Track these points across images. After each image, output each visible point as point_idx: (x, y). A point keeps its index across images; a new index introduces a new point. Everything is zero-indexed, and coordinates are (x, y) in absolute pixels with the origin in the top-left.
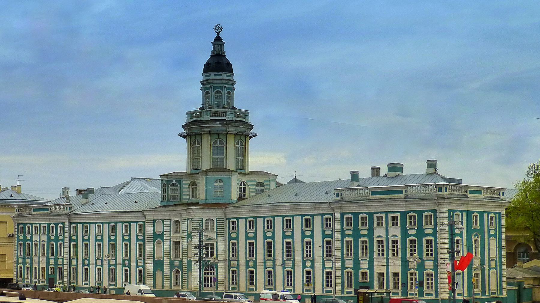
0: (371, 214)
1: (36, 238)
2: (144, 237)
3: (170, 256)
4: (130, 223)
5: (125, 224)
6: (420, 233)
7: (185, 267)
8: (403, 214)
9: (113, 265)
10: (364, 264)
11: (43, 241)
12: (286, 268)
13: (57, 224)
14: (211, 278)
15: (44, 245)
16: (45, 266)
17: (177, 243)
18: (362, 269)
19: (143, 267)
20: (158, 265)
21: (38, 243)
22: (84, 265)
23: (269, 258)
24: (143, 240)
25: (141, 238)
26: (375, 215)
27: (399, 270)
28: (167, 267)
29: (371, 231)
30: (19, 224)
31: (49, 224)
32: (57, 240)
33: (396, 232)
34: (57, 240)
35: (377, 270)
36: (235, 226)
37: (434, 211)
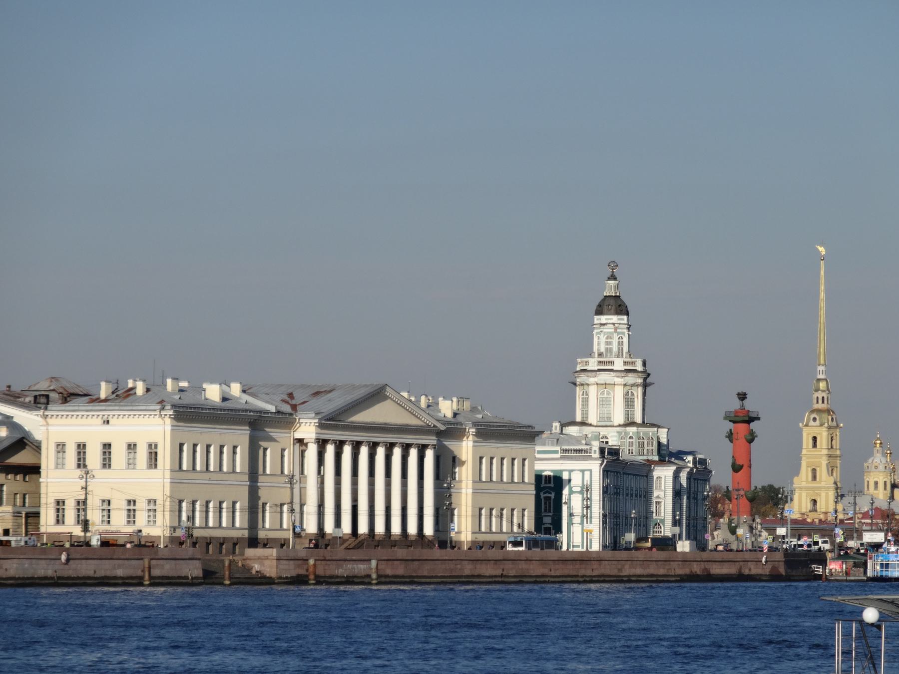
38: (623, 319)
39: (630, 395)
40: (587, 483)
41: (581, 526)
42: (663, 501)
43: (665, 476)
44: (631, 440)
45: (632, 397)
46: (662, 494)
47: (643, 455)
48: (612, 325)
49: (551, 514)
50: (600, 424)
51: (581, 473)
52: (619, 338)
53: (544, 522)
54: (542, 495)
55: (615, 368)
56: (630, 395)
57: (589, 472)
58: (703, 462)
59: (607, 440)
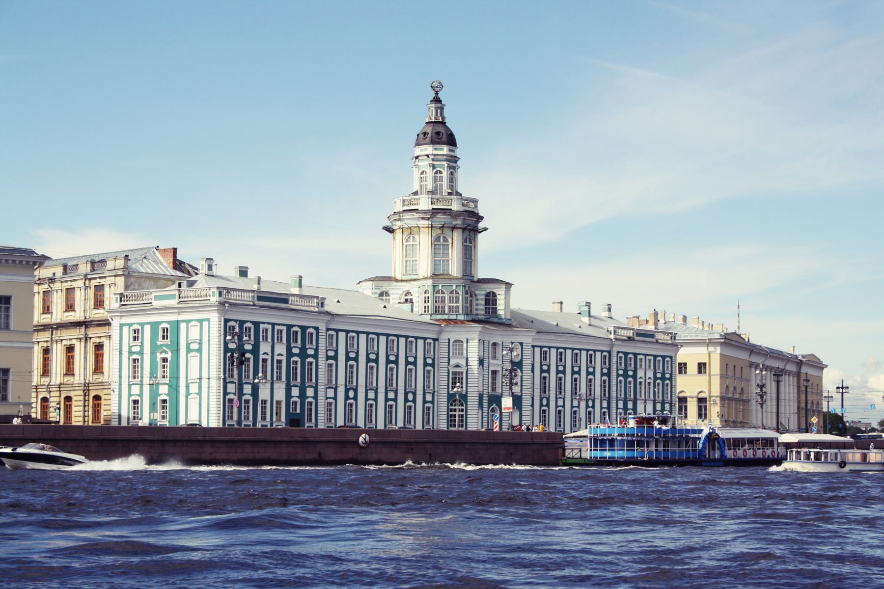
0: (635, 355)
1: (265, 348)
2: (434, 360)
4: (416, 338)
9: (391, 400)
11: (279, 355)
13: (304, 328)
15: (279, 362)
17: (494, 373)
18: (629, 409)
19: (432, 402)
21: (269, 357)
23: (560, 396)
24: (433, 365)
25: (429, 361)
26: (639, 357)
29: (635, 372)
31: (289, 327)
32: (303, 355)
34: (303, 355)
37: (671, 357)
38: (442, 149)
39: (442, 240)
40: (789, 379)
41: (198, 397)
42: (465, 372)
44: (427, 295)
45: (444, 243)
46: (463, 362)
47: (443, 313)
48: (426, 157)
49: (168, 382)
50: (405, 278)
52: (436, 173)
53: (160, 393)
54: (159, 356)
55: (420, 208)
56: (442, 240)
57: (207, 322)
58: (731, 341)
59: (411, 297)
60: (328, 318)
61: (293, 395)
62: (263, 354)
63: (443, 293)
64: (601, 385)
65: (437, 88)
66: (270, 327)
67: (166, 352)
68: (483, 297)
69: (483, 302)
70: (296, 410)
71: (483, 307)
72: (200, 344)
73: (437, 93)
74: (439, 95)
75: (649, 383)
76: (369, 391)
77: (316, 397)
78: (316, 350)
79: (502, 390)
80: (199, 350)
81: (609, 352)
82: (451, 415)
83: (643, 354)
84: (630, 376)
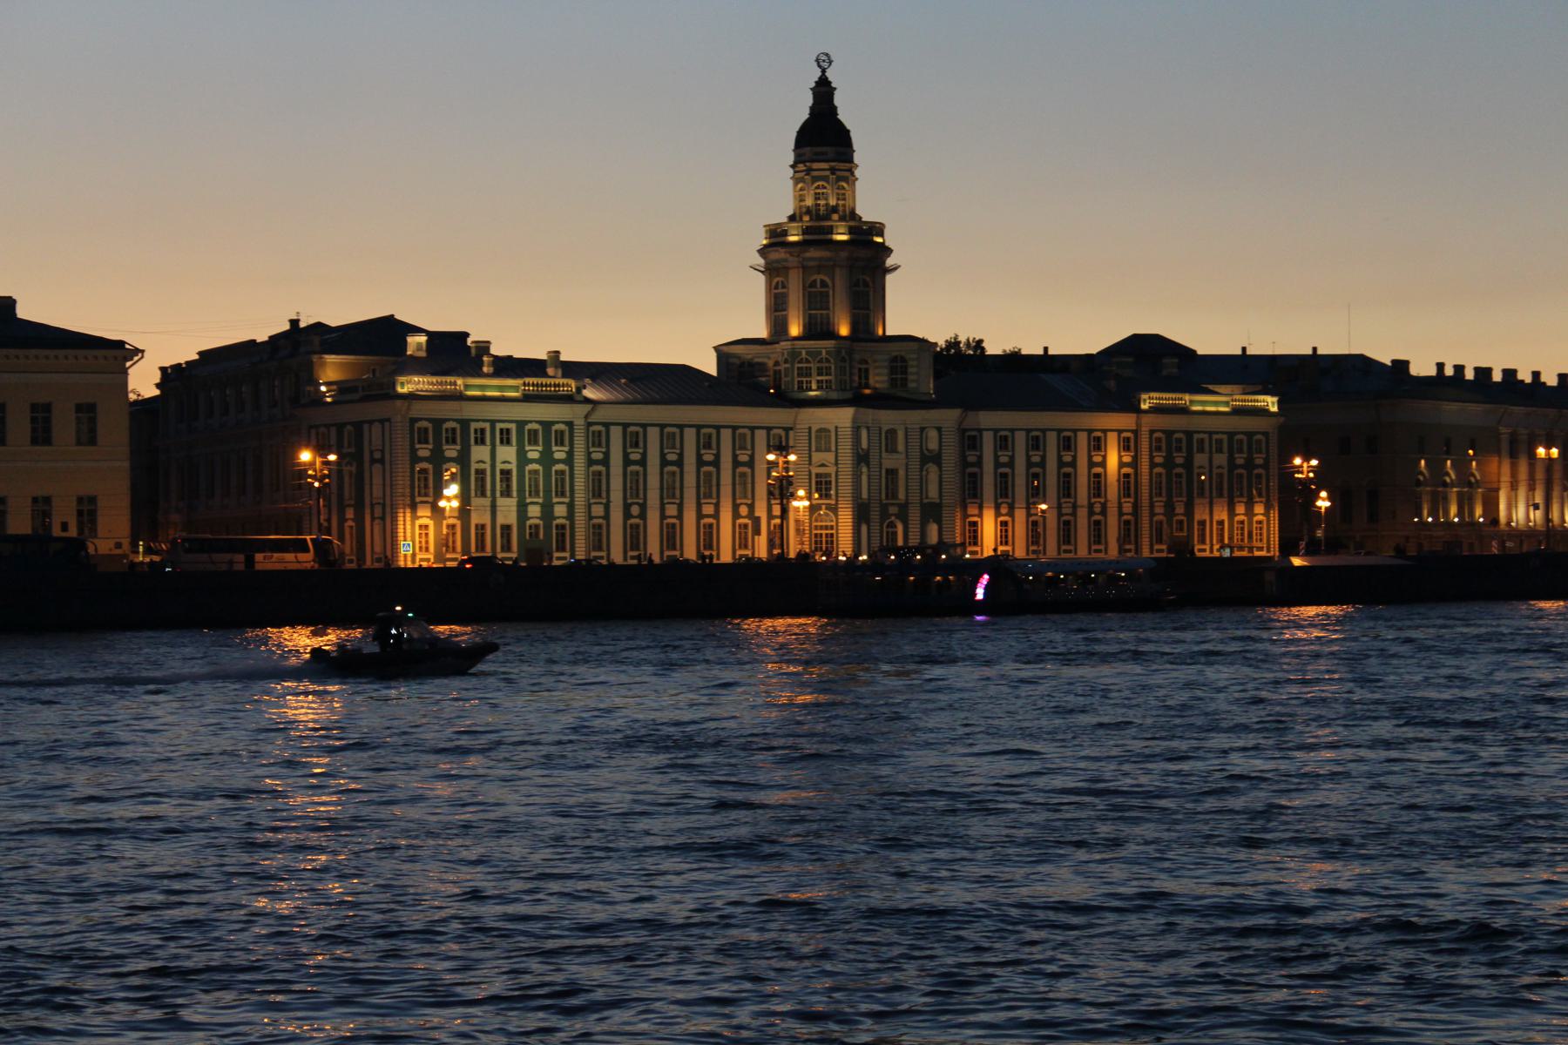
1: (480, 453)
3: (880, 497)
5: (741, 431)
6: (1249, 461)
7: (915, 515)
8: (1231, 435)
10: (1180, 509)
11: (504, 462)
12: (1063, 515)
13: (547, 425)
14: (827, 534)
15: (506, 474)
16: (512, 519)
17: (892, 473)
20: (862, 514)
21: (487, 467)
22: (627, 514)
26: (1196, 436)
27: (1224, 516)
28: (875, 515)
30: (414, 421)
33: (1221, 459)
34: (547, 459)
35: (1197, 517)
36: (970, 441)
37: (1266, 434)
43: (836, 427)
51: (380, 426)
60: (588, 407)
61: (530, 515)
62: (478, 462)
63: (807, 361)
64: (1119, 481)
65: (824, 61)
66: (487, 426)
67: (351, 465)
68: (886, 364)
69: (886, 371)
70: (537, 534)
71: (886, 378)
72: (383, 451)
73: (824, 71)
74: (830, 74)
75: (1220, 476)
76: (667, 506)
77: (571, 515)
78: (570, 454)
79: (907, 496)
80: (382, 461)
81: (1136, 432)
82: (816, 535)
83: (1205, 432)
84: (1178, 466)
